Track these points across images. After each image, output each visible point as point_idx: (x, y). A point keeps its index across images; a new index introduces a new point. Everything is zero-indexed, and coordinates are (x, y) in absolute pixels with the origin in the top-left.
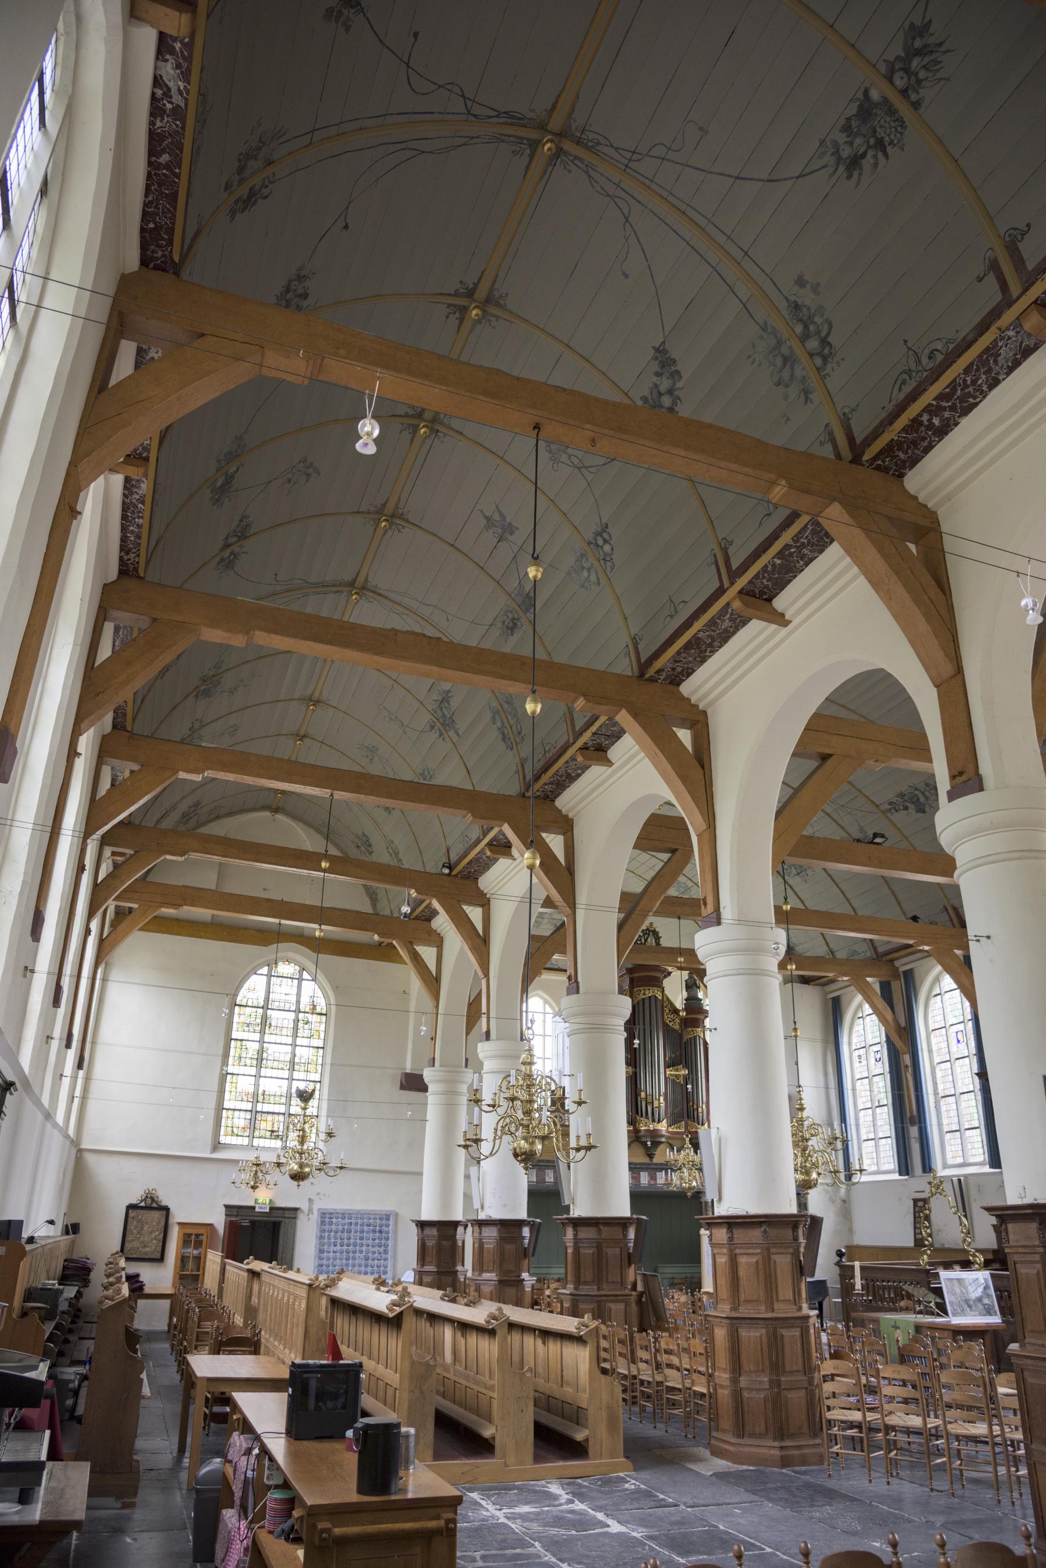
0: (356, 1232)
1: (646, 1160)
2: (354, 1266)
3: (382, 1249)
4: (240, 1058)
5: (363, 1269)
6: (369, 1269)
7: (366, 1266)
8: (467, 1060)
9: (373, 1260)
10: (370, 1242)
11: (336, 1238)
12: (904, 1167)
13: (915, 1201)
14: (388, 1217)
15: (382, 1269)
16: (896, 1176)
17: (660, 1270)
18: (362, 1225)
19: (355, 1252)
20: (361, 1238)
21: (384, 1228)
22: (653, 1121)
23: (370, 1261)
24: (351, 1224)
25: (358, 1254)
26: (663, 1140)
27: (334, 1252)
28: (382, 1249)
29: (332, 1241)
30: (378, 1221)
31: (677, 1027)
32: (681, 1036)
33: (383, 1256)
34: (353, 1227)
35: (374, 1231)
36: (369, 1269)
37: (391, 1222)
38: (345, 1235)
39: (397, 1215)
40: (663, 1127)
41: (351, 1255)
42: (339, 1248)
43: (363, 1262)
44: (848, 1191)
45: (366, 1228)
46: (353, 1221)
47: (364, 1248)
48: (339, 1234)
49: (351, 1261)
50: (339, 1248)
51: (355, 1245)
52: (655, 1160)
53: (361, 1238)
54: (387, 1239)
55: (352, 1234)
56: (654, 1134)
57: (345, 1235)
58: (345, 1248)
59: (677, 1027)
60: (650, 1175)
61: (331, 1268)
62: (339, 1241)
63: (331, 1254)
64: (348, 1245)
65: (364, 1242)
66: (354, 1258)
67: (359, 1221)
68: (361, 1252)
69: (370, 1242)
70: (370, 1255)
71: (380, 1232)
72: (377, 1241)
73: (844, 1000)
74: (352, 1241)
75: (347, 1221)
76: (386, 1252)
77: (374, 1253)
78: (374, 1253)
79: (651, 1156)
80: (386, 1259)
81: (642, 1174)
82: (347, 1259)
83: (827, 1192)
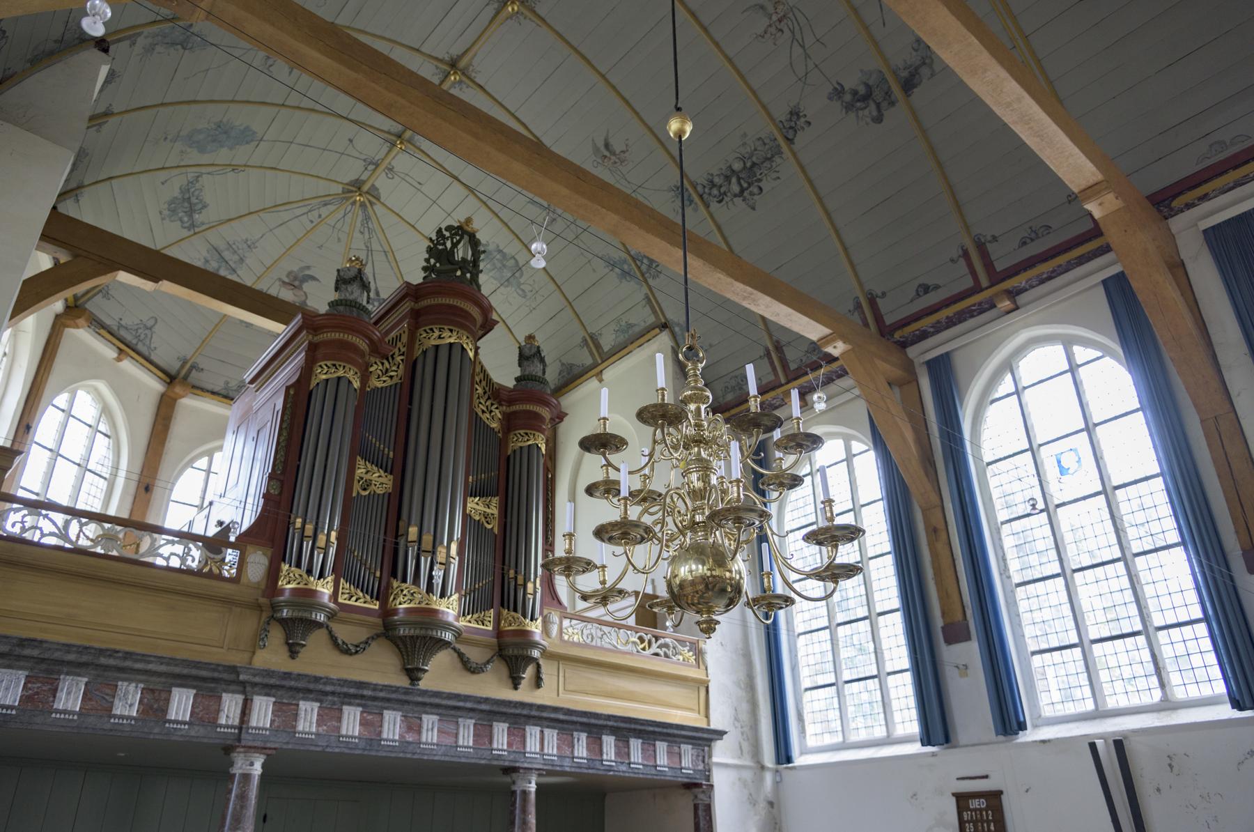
1: (404, 682)
12: (937, 724)
13: (962, 799)
16: (916, 748)
22: (430, 589)
31: (494, 425)
32: (503, 443)
40: (450, 608)
44: (777, 784)
52: (423, 684)
56: (429, 617)
79: (413, 674)
81: (388, 715)
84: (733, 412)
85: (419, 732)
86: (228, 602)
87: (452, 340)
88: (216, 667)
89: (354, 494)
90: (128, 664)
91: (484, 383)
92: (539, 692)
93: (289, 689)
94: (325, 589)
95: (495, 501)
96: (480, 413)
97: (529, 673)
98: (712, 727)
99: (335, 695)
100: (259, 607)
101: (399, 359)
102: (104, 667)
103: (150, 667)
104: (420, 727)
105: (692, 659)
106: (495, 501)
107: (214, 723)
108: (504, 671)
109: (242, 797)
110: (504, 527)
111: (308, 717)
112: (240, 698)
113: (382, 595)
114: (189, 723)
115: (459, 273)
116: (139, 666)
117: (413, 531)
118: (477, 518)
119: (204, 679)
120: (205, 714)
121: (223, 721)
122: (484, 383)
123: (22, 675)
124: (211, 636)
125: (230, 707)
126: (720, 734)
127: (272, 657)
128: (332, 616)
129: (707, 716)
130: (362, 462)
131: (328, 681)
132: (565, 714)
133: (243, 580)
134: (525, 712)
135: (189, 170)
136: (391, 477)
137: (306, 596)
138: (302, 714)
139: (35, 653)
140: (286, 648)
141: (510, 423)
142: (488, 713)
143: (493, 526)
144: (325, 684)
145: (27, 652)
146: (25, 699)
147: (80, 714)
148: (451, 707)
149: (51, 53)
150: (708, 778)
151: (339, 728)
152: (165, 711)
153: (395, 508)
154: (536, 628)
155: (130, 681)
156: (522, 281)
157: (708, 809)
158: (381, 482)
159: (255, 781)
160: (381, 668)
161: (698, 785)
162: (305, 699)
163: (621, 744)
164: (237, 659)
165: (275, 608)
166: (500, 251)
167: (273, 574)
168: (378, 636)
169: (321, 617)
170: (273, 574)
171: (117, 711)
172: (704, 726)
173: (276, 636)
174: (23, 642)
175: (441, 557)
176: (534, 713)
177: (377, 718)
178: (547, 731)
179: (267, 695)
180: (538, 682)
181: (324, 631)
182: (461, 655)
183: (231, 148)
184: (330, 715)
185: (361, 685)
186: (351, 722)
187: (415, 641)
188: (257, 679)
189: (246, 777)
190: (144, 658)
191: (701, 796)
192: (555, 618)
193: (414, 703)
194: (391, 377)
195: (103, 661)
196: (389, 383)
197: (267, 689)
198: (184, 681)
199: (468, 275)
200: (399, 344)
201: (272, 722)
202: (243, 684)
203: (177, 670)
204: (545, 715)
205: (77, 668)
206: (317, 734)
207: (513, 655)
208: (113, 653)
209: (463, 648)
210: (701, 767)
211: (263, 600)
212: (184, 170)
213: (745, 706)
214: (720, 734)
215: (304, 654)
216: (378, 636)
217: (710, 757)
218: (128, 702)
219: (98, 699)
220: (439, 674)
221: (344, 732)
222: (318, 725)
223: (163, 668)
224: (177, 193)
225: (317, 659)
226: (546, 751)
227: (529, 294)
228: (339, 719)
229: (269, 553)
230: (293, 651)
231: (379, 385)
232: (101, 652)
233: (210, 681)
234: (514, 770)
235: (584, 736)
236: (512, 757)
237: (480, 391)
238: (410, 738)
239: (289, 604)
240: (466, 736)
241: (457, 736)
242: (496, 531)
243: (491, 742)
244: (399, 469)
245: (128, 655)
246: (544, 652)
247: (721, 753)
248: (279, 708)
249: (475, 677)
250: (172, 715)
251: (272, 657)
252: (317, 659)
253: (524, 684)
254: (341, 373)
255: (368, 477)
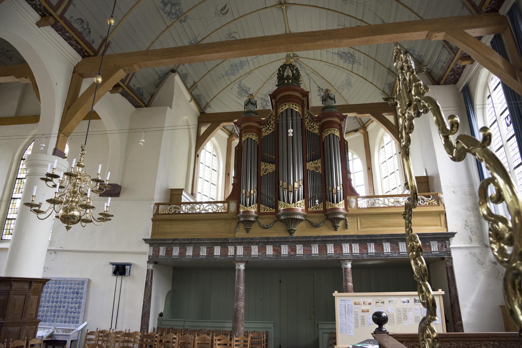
0: (62, 293)
1: (287, 235)
2: (58, 317)
3: (77, 306)
4: (20, 188)
5: (63, 319)
6: (68, 319)
7: (66, 317)
8: (55, 150)
9: (71, 313)
10: (70, 300)
11: (50, 297)
14: (83, 283)
15: (76, 319)
17: (320, 326)
18: (66, 289)
19: (60, 307)
20: (65, 298)
21: (80, 291)
23: (69, 314)
24: (60, 287)
25: (62, 309)
26: (299, 217)
27: (48, 307)
28: (77, 306)
29: (47, 299)
30: (77, 286)
31: (316, 131)
32: (320, 137)
33: (77, 310)
34: (61, 290)
35: (73, 293)
36: (68, 319)
37: (85, 286)
38: (56, 295)
39: (89, 281)
40: (300, 207)
41: (58, 309)
42: (50, 304)
43: (64, 314)
45: (68, 290)
46: (61, 285)
47: (66, 304)
48: (52, 294)
49: (57, 313)
50: (50, 304)
51: (61, 302)
52: (295, 235)
53: (65, 298)
54: (81, 298)
55: (60, 294)
56: (289, 212)
57: (56, 295)
58: (54, 304)
59: (316, 131)
60: (290, 247)
61: (44, 318)
62: (51, 299)
63: (46, 308)
64: (57, 302)
65: (67, 300)
66: (59, 312)
67: (65, 286)
68: (64, 307)
69: (70, 300)
70: (69, 309)
71: (77, 293)
72: (75, 300)
73: (471, 86)
74: (59, 299)
75: (58, 285)
76: (79, 307)
77: (72, 308)
78: (72, 308)
80: (79, 313)
82: (55, 312)
83: (474, 255)
84: (444, 78)
85: (296, 251)
86: (225, 219)
87: (286, 108)
88: (222, 239)
89: (262, 175)
90: (199, 241)
91: (309, 117)
92: (347, 230)
93: (247, 243)
94: (253, 210)
95: (319, 160)
96: (309, 129)
97: (341, 224)
98: (449, 231)
99: (263, 243)
100: (234, 219)
101: (272, 122)
102: (196, 243)
103: (205, 242)
104: (296, 249)
105: (435, 203)
106: (319, 160)
107: (227, 255)
108: (330, 223)
109: (239, 276)
110: (324, 170)
111: (255, 251)
112: (233, 247)
113: (276, 207)
114: (220, 256)
115: (286, 82)
116: (202, 242)
117: (281, 182)
118: (312, 169)
119: (222, 243)
120: (224, 252)
121: (229, 254)
122: (309, 117)
123: (178, 248)
124: (221, 231)
125: (231, 251)
126: (453, 234)
127: (241, 233)
128: (257, 218)
129: (447, 227)
130: (263, 163)
131: (256, 239)
132: (357, 237)
133: (230, 212)
134: (338, 239)
135: (236, 81)
136: (274, 165)
137: (246, 212)
138: (253, 250)
139: (177, 242)
140: (245, 230)
141: (322, 129)
142: (323, 242)
143: (320, 170)
144: (256, 240)
145: (176, 242)
146: (180, 254)
147: (192, 256)
148: (307, 242)
149: (161, 82)
150: (450, 254)
151: (265, 253)
152: (213, 253)
153: (276, 176)
154: (341, 206)
155: (203, 246)
156: (357, 59)
157: (452, 268)
158: (271, 168)
159: (242, 271)
160: (278, 232)
161: (443, 259)
162: (253, 245)
163: (394, 245)
164: (230, 236)
165: (239, 218)
166: (344, 53)
167: (238, 208)
168: (276, 221)
169: (253, 219)
170: (238, 208)
171: (201, 254)
172: (445, 231)
173: (242, 226)
174: (174, 240)
175: (291, 188)
176: (342, 239)
177: (279, 248)
178: (353, 245)
179: (240, 245)
180: (346, 226)
181: (257, 223)
182: (310, 222)
183: (242, 69)
184: (262, 249)
185: (268, 238)
186: (270, 250)
187: (289, 220)
188: (234, 241)
189: (239, 270)
190: (202, 239)
191: (448, 263)
192: (353, 200)
193: (292, 243)
194: (270, 130)
195: (193, 242)
196: (270, 132)
197: (240, 244)
198: (217, 244)
199: (290, 81)
200: (272, 117)
201: (244, 253)
202: (232, 243)
203: (212, 241)
204: (347, 239)
205: (189, 244)
206: (258, 255)
207: (332, 218)
208: (194, 239)
209: (310, 220)
210: (445, 250)
211: (234, 217)
212: (234, 82)
213: (472, 219)
214: (453, 234)
215: (251, 231)
216: (276, 221)
217: (450, 245)
218: (203, 252)
219: (196, 252)
220: (301, 230)
221: (267, 254)
222: (259, 252)
223: (208, 241)
224: (238, 90)
225: (256, 232)
226: (353, 252)
227: (362, 63)
228: (265, 250)
229: (236, 202)
230: (248, 231)
231: (266, 134)
232: (192, 239)
233: (224, 243)
234: (339, 260)
235: (373, 245)
236: (336, 256)
237: (308, 120)
238: (292, 253)
239: (242, 216)
240: (315, 250)
241: (311, 251)
242: (321, 172)
243: (326, 252)
244: (276, 162)
245: (198, 239)
246: (346, 215)
247: (454, 243)
248: (245, 249)
249: (317, 229)
250: (215, 254)
251: (241, 233)
252: (256, 232)
253: (339, 229)
254: (247, 136)
255: (265, 168)
